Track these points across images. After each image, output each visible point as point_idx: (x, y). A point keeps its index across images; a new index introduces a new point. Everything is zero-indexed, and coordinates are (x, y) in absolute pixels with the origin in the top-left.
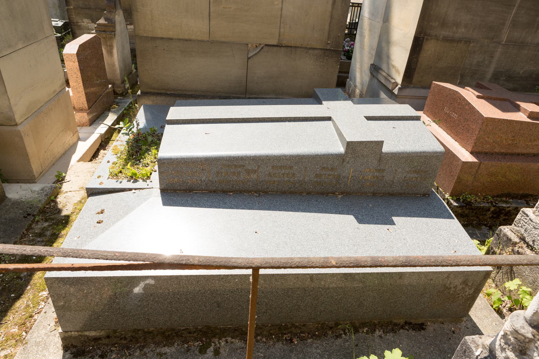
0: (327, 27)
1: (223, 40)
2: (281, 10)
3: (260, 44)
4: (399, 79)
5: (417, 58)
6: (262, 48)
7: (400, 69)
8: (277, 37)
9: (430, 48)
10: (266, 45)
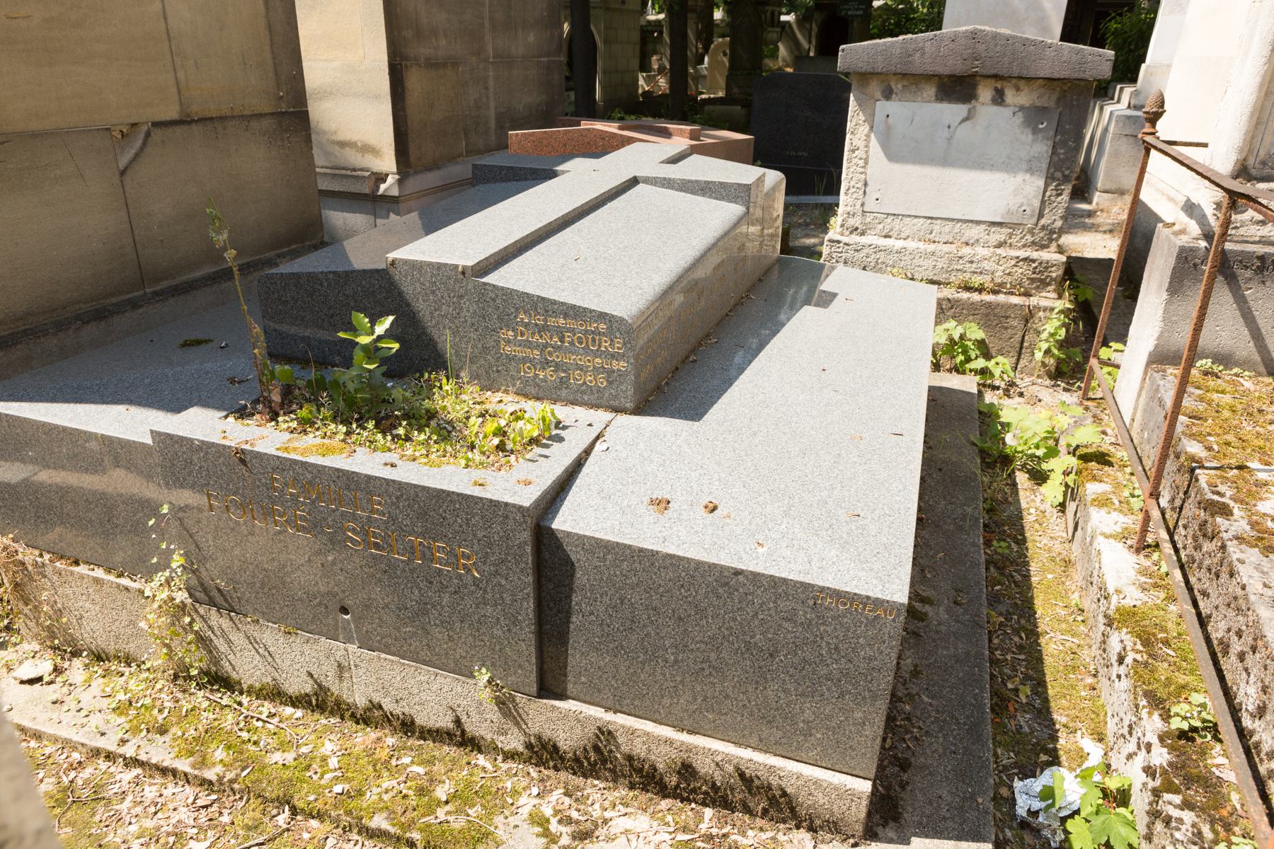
0: (268, 55)
1: (34, 126)
2: (165, 18)
3: (134, 125)
4: (387, 163)
5: (404, 110)
6: (148, 134)
7: (372, 140)
8: (176, 97)
9: (415, 81)
10: (157, 124)
